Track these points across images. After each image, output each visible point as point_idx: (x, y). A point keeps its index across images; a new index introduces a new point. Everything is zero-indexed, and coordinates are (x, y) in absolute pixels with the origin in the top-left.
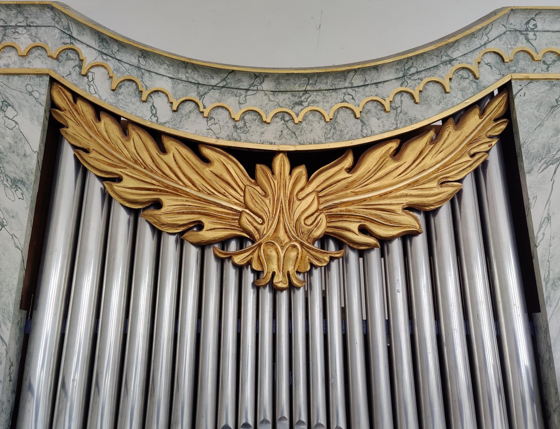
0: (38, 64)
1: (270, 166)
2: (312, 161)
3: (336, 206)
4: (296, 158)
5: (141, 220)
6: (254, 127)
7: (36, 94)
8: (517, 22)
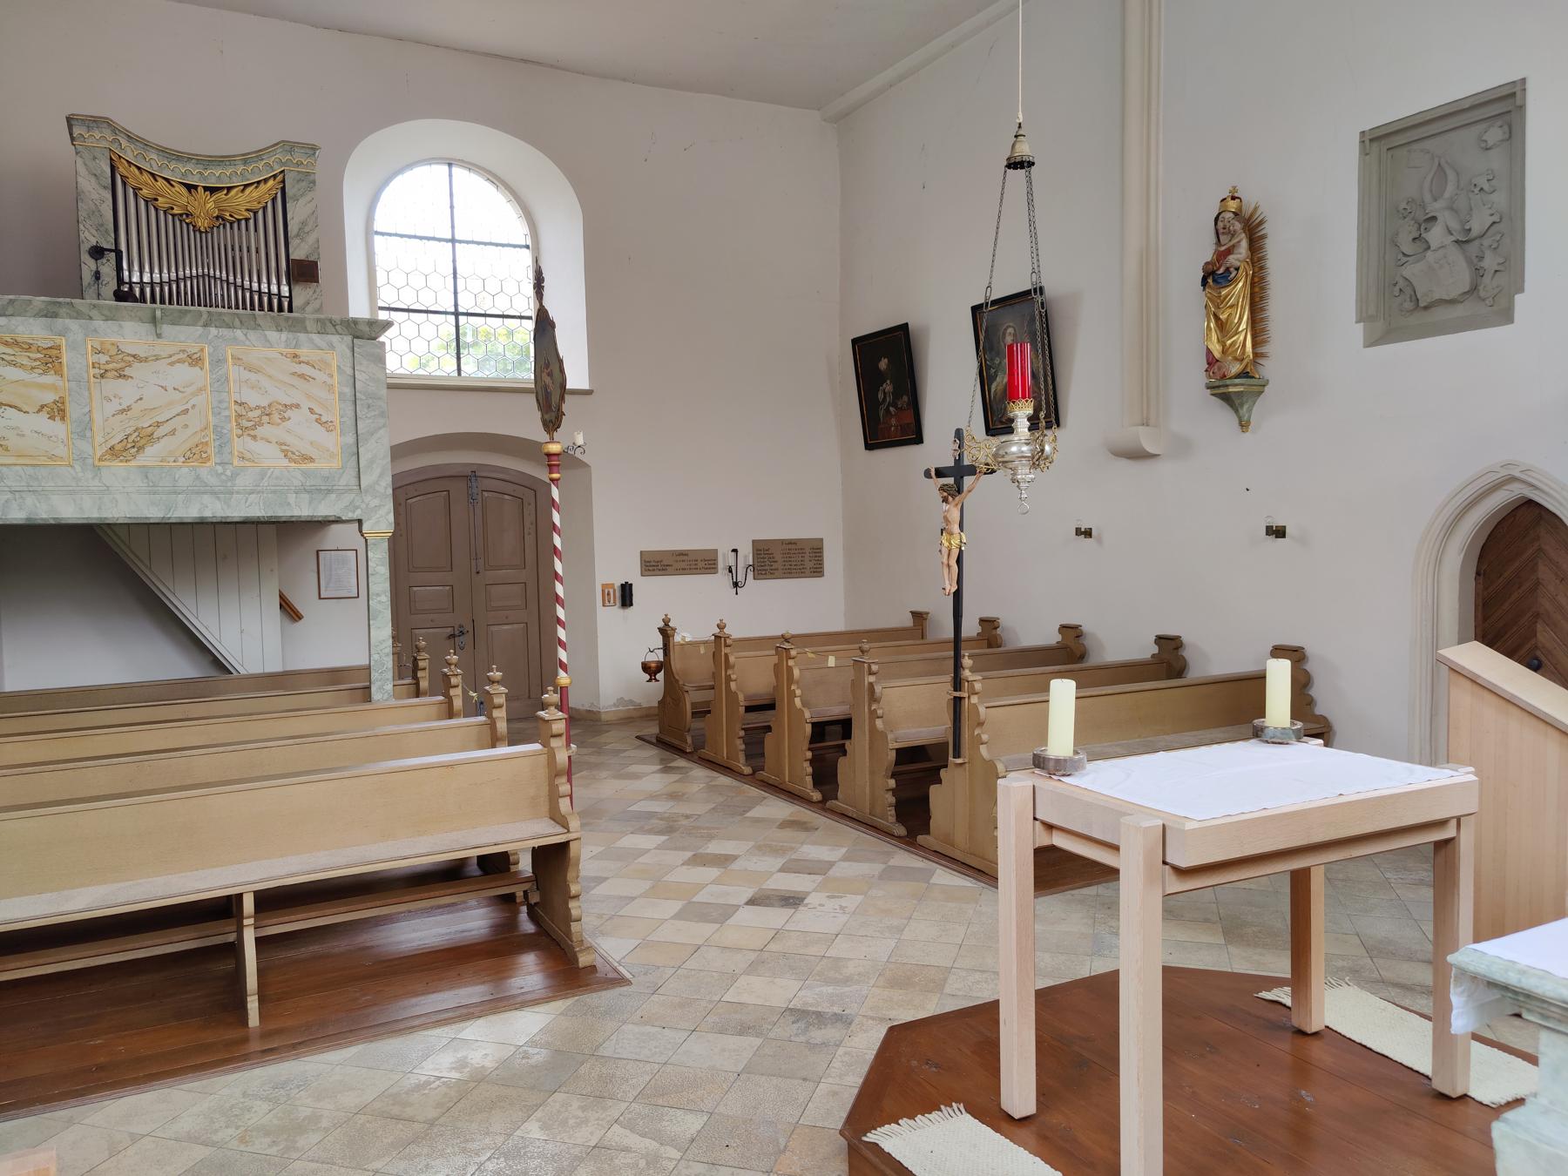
0: (104, 144)
2: (212, 190)
4: (206, 189)
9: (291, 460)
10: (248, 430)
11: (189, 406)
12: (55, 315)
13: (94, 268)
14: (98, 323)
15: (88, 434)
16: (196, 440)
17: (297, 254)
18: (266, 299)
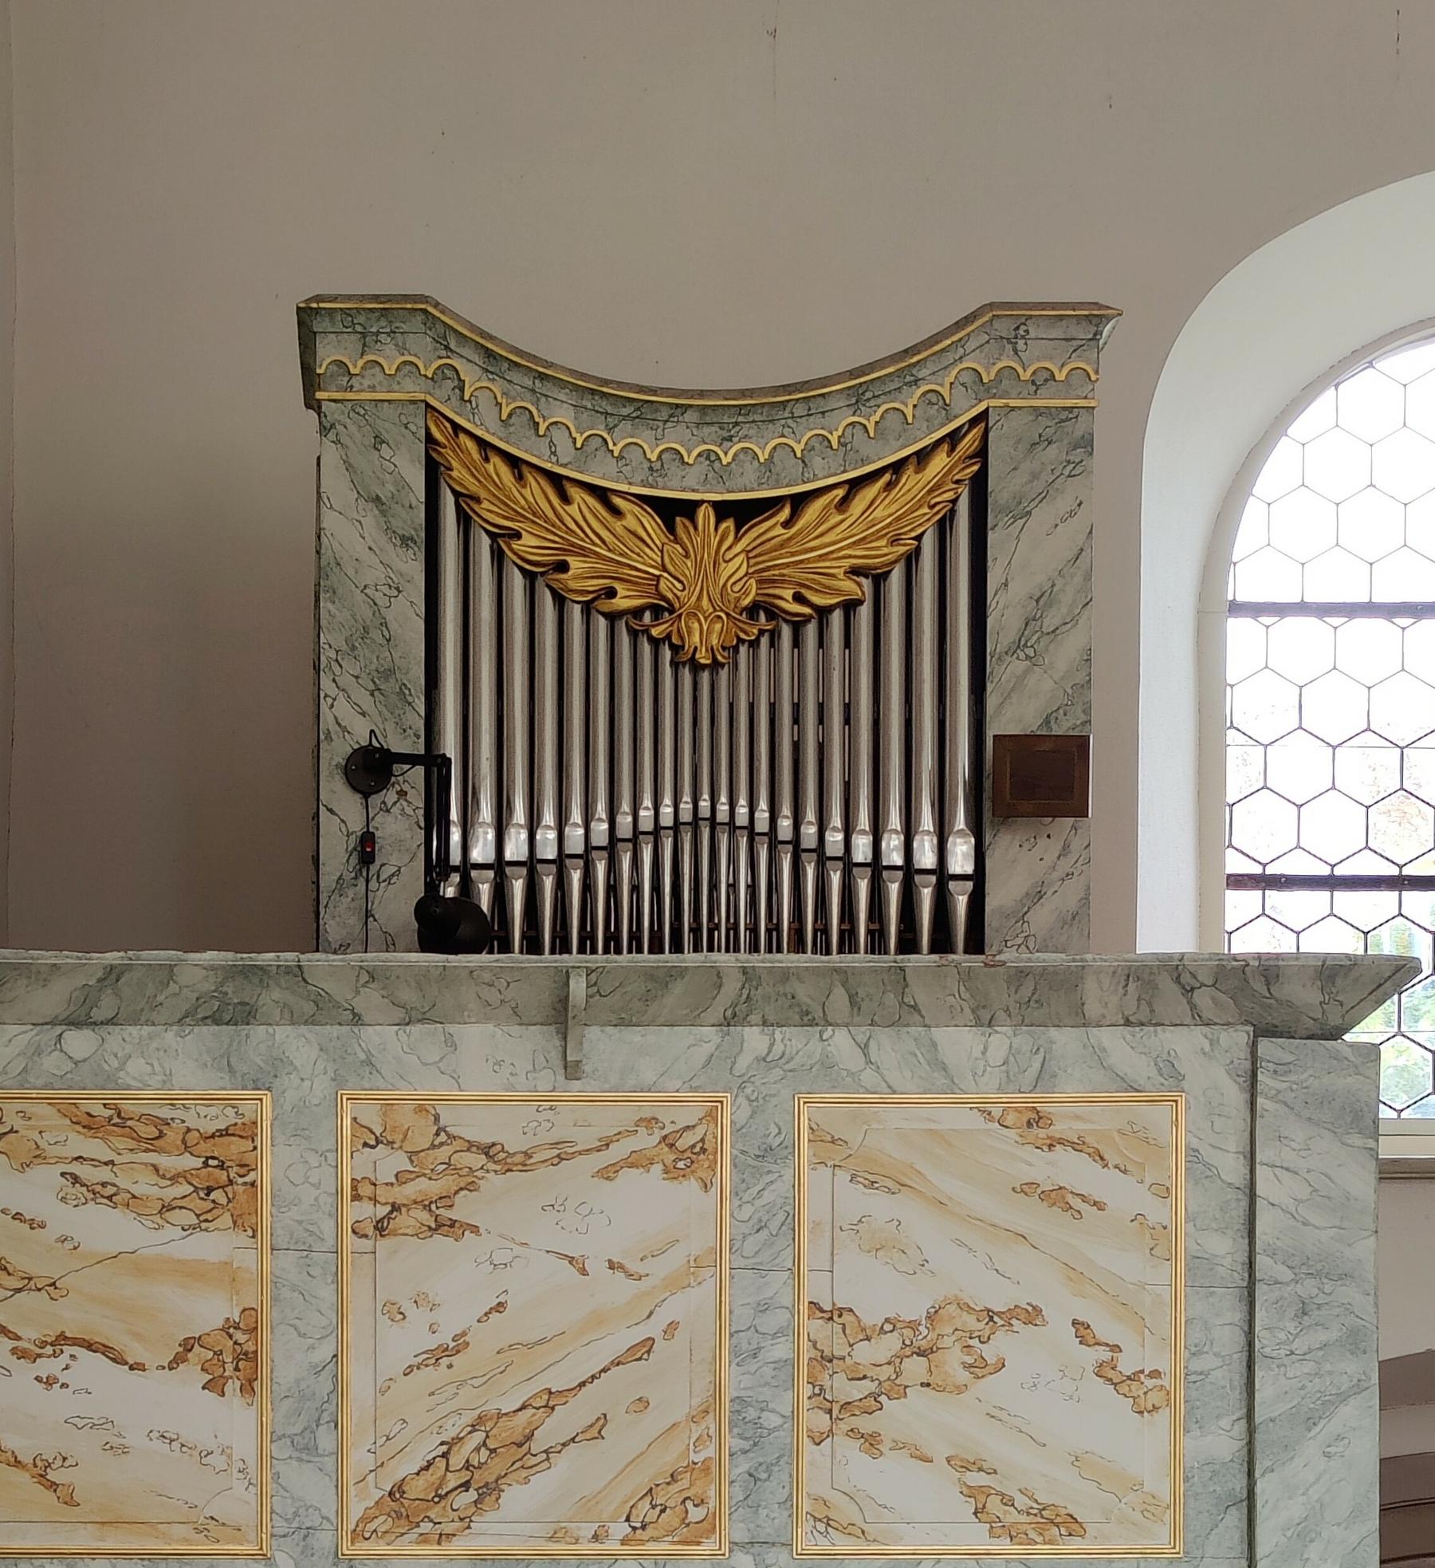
0: (411, 389)
1: (693, 519)
2: (742, 513)
3: (768, 569)
4: (722, 510)
5: (540, 583)
6: (674, 469)
7: (412, 427)
8: (1004, 328)
9: (998, 1527)
10: (852, 1416)
11: (654, 1329)
12: (246, 1015)
13: (357, 826)
14: (381, 1037)
15: (325, 1440)
16: (670, 1457)
17: (1015, 714)
18: (894, 889)
